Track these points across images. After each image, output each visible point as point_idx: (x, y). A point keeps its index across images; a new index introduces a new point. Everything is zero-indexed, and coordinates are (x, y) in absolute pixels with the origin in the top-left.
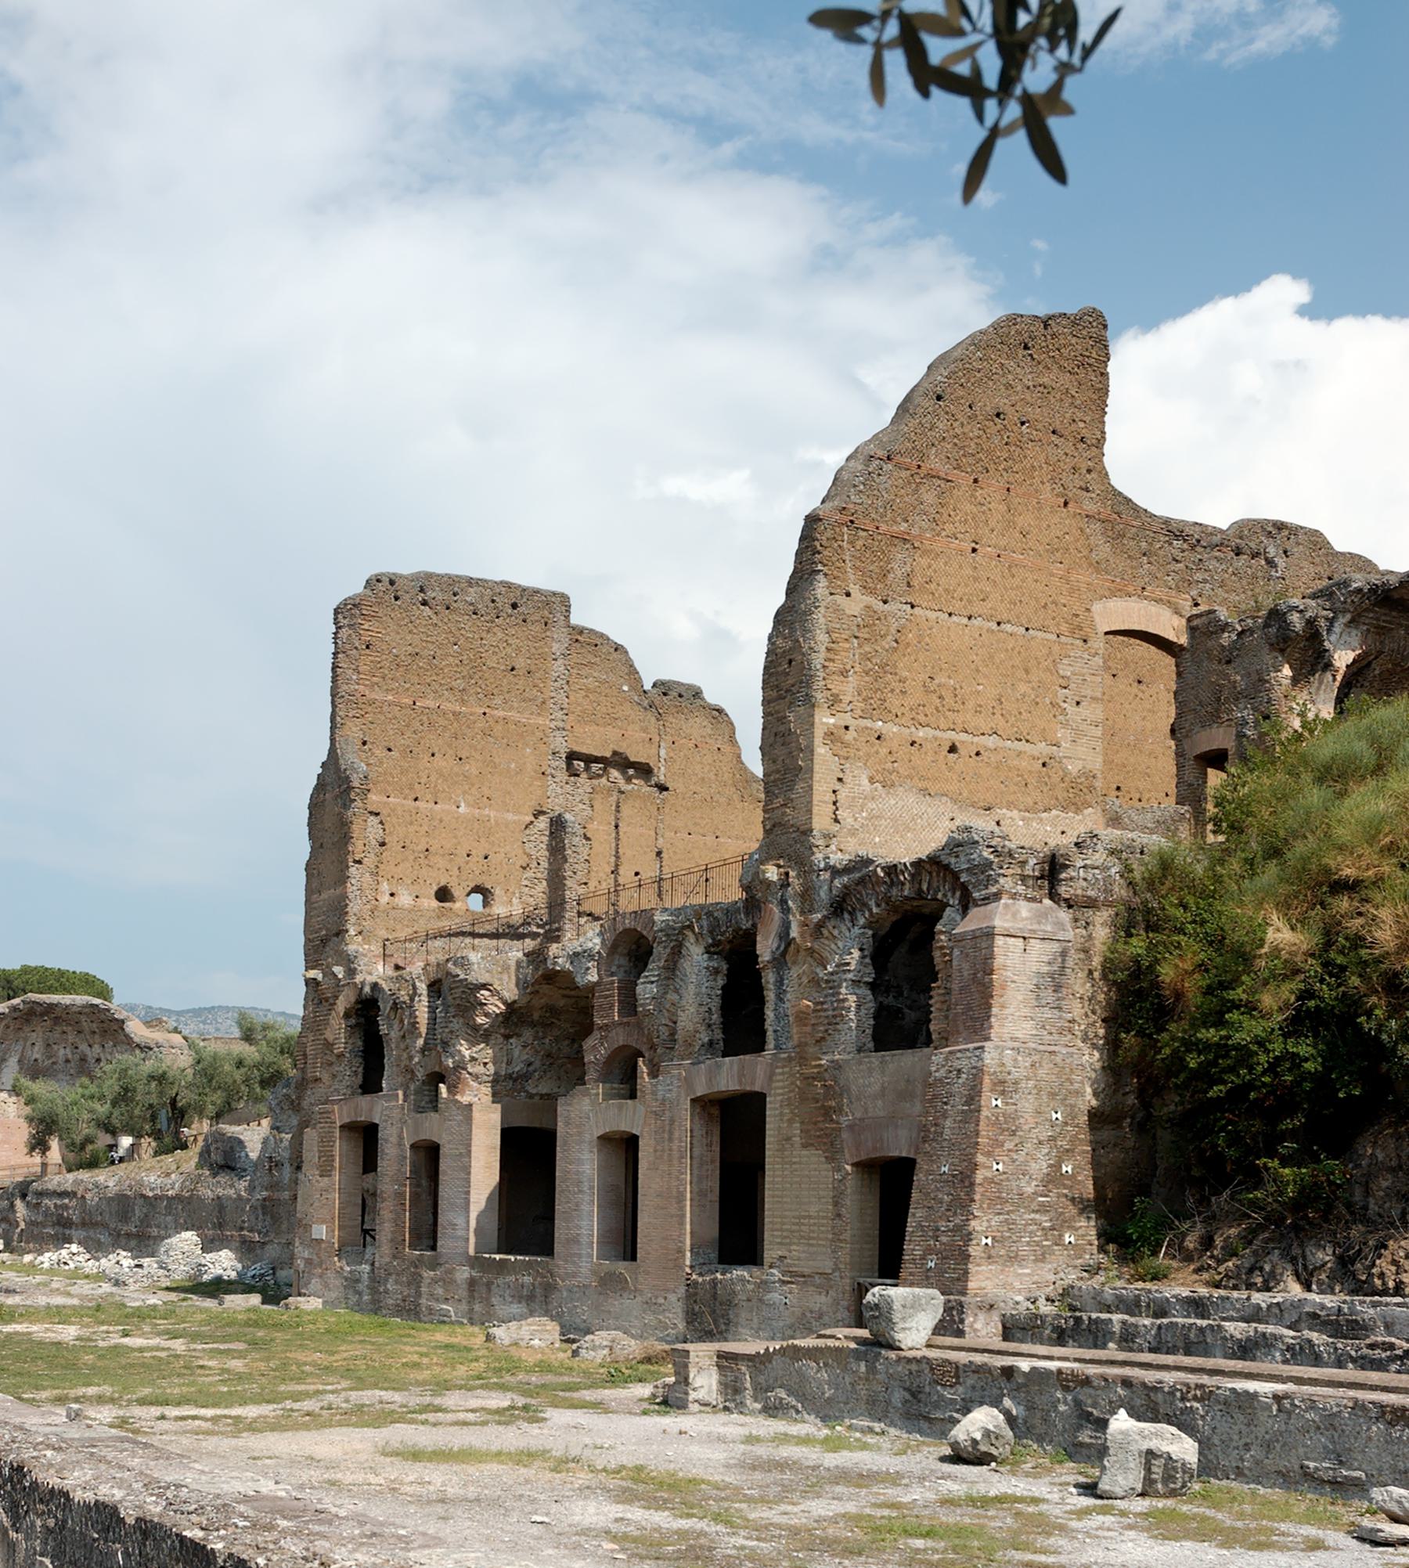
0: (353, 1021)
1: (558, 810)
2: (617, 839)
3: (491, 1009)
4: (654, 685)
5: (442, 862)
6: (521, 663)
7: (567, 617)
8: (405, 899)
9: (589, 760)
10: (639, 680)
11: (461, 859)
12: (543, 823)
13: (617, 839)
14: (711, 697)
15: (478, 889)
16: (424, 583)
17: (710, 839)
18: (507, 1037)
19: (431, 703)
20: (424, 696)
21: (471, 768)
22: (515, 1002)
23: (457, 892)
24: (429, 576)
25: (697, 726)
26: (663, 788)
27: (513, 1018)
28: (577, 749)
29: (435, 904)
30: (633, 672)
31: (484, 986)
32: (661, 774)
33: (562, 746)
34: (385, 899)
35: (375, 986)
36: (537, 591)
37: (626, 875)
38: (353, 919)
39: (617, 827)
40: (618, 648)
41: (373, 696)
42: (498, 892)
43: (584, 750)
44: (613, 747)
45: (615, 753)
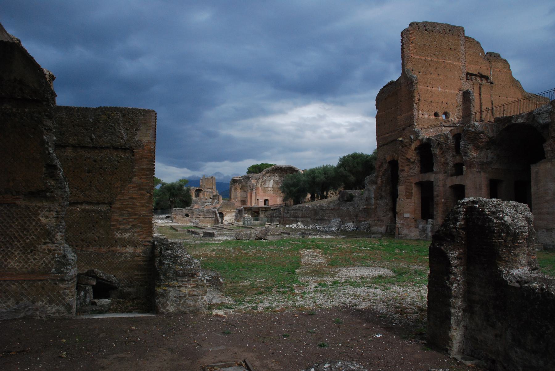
0: (417, 151)
1: (465, 90)
2: (480, 98)
3: (484, 140)
4: (487, 53)
5: (434, 105)
6: (452, 47)
7: (464, 34)
8: (426, 116)
9: (472, 75)
10: (483, 52)
11: (440, 104)
12: (461, 93)
13: (480, 98)
14: (503, 57)
15: (445, 113)
16: (425, 24)
17: (505, 98)
18: (487, 149)
19: (430, 59)
20: (427, 57)
21: (441, 77)
22: (492, 137)
23: (440, 114)
24: (426, 22)
25: (500, 65)
26: (492, 83)
27: (491, 143)
28: (469, 72)
29: (434, 117)
30: (482, 49)
31: (483, 132)
32: (491, 79)
33: (465, 71)
34: (421, 116)
35: (429, 139)
36: (455, 26)
37: (484, 108)
38: (416, 121)
39: (480, 95)
40: (478, 43)
41: (414, 57)
42: (451, 114)
43: (471, 72)
44: (478, 71)
45: (479, 73)
